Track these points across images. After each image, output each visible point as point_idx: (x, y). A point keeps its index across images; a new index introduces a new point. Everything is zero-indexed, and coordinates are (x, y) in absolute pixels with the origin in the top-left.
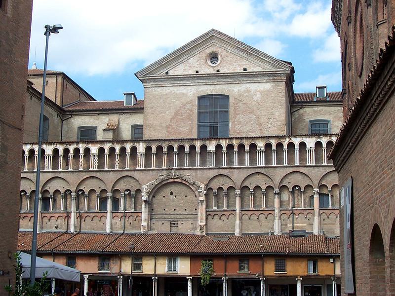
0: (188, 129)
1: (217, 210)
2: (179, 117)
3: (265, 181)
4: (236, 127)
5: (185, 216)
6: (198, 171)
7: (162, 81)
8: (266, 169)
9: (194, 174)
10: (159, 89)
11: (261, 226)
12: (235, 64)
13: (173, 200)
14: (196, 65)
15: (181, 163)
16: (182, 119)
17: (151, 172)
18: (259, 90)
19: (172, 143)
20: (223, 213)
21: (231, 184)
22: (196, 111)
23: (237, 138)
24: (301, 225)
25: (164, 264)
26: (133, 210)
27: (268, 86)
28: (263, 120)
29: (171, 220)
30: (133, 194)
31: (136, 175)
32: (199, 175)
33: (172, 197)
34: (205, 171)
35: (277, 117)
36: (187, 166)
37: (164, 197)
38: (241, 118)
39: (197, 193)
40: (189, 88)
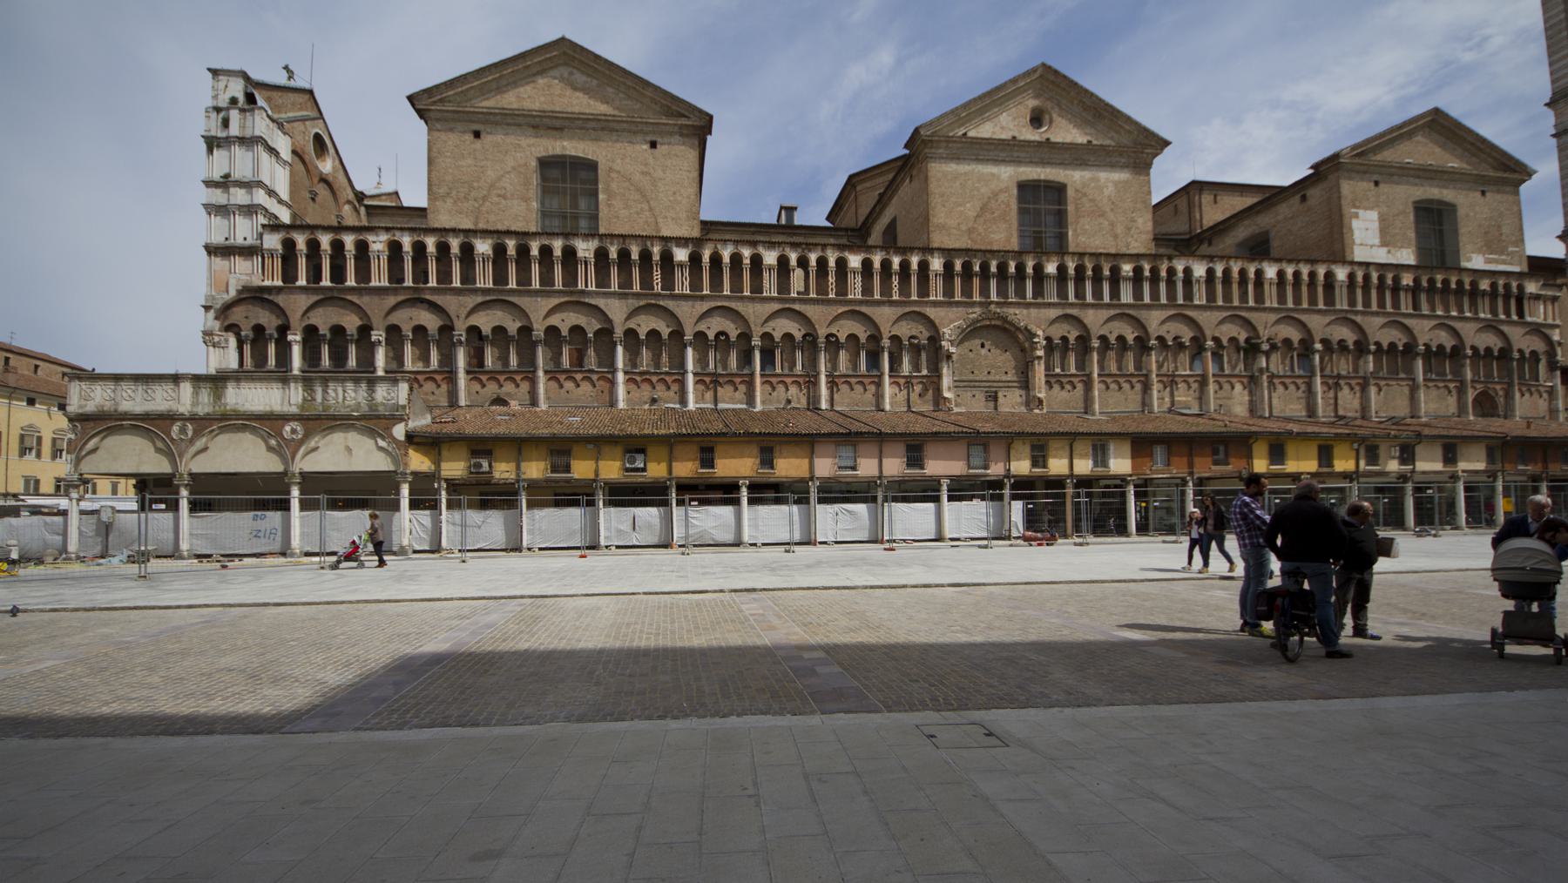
0: (1004, 235)
2: (988, 216)
5: (1006, 384)
11: (1126, 399)
13: (986, 357)
14: (1011, 127)
15: (1002, 292)
16: (994, 218)
22: (1014, 206)
24: (1184, 399)
28: (1119, 230)
31: (931, 312)
33: (983, 351)
35: (1140, 226)
38: (1086, 224)
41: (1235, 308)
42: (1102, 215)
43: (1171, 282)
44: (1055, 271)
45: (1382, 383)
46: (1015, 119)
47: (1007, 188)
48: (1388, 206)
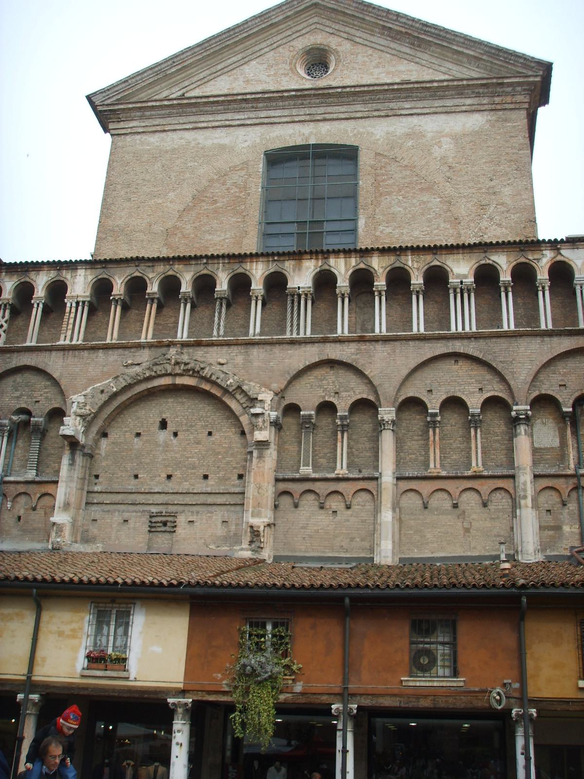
1: (313, 475)
4: (381, 228)
5: (202, 499)
6: (255, 351)
7: (163, 117)
8: (482, 343)
9: (240, 359)
11: (467, 530)
13: (166, 445)
14: (263, 77)
16: (216, 211)
17: (101, 353)
18: (447, 130)
19: (178, 267)
20: (333, 487)
21: (361, 392)
23: (384, 251)
25: (74, 634)
26: (31, 475)
27: (476, 121)
28: (463, 209)
29: (154, 509)
30: (36, 424)
31: (55, 364)
32: (256, 364)
33: (163, 436)
34: (277, 350)
35: (508, 201)
37: (138, 435)
39: (244, 419)
40: (242, 131)
42: (430, 188)
47: (246, 163)
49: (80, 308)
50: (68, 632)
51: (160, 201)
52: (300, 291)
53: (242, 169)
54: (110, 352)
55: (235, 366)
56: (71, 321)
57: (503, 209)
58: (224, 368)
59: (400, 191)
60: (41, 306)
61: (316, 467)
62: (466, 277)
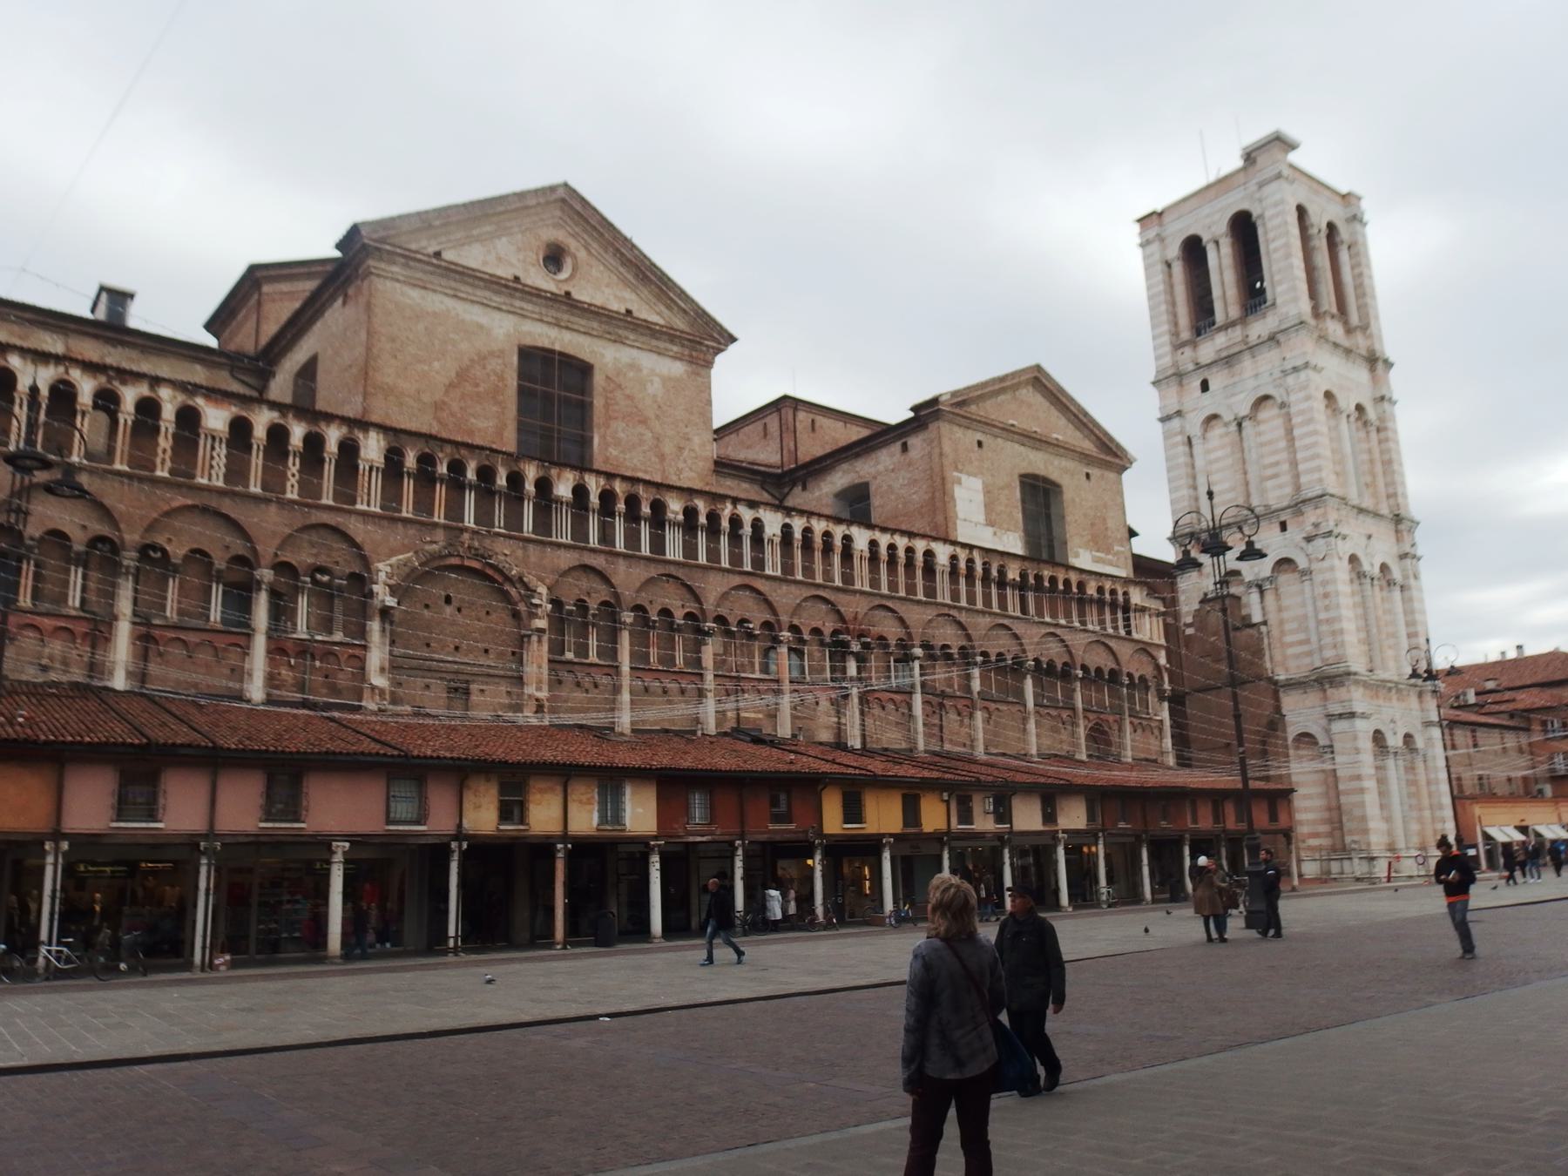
1: (576, 660)
2: (469, 388)
3: (682, 600)
6: (531, 547)
7: (425, 272)
8: (686, 570)
9: (520, 553)
10: (415, 294)
12: (607, 291)
14: (514, 261)
15: (484, 517)
16: (478, 394)
22: (512, 381)
24: (753, 715)
25: (589, 802)
28: (668, 448)
29: (449, 677)
31: (355, 528)
33: (448, 610)
35: (697, 449)
36: (500, 527)
38: (620, 428)
40: (497, 316)
41: (818, 586)
43: (735, 538)
44: (570, 496)
45: (992, 706)
46: (519, 250)
47: (502, 352)
48: (992, 475)
49: (374, 474)
50: (585, 800)
51: (426, 368)
52: (564, 500)
53: (499, 357)
54: (409, 526)
55: (516, 558)
56: (366, 485)
57: (694, 455)
58: (508, 559)
59: (624, 418)
60: (333, 461)
61: (576, 655)
62: (677, 513)
